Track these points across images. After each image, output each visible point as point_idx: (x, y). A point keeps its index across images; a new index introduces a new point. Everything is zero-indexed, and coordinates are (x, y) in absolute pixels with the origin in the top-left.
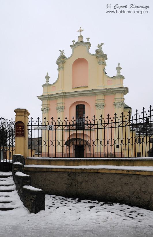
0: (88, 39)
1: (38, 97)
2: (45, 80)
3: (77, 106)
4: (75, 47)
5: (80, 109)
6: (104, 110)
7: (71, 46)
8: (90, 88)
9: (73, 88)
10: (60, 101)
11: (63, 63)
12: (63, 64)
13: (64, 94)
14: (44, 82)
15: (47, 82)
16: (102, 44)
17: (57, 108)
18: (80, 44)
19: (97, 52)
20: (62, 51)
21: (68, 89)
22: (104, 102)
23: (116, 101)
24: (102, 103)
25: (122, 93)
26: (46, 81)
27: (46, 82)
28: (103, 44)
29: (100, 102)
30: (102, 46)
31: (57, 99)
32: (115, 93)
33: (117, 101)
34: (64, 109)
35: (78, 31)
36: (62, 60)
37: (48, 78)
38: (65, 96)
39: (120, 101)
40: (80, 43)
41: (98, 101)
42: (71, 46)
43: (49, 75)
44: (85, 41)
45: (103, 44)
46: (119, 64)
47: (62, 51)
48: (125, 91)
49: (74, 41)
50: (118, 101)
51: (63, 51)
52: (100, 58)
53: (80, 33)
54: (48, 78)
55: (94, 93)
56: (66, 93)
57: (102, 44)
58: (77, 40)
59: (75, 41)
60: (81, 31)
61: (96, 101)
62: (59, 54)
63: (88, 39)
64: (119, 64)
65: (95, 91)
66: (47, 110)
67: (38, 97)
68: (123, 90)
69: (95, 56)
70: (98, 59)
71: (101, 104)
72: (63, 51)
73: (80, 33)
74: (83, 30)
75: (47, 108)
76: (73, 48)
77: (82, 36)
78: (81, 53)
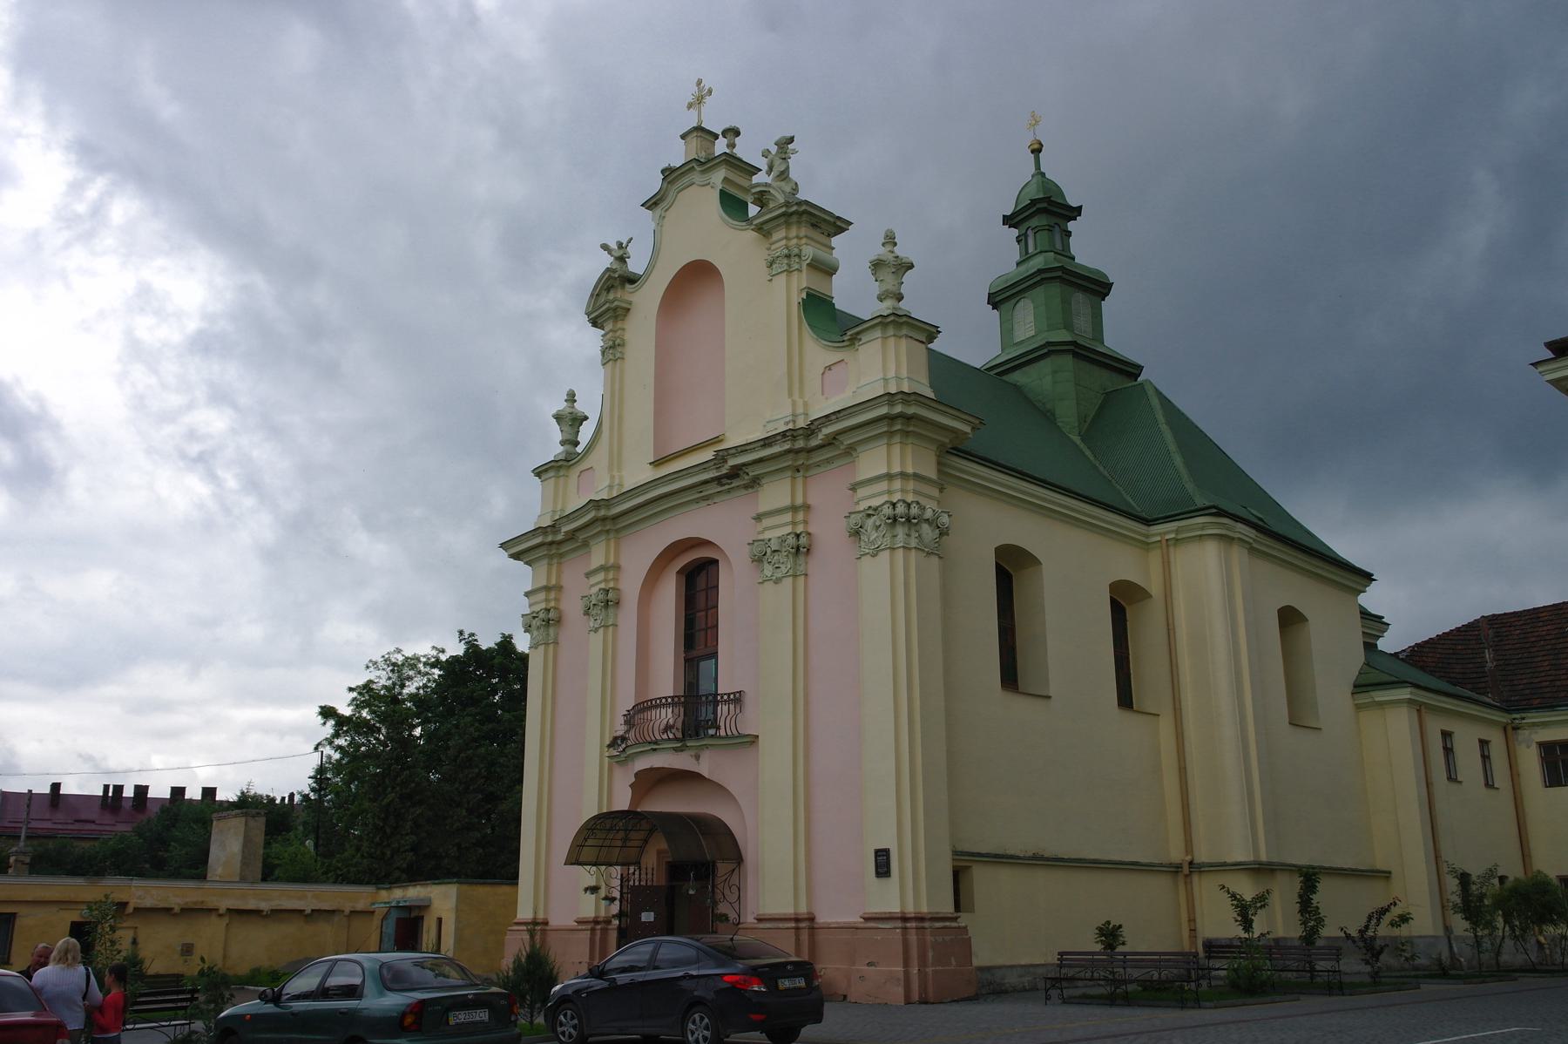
4: (664, 205)
6: (801, 579)
12: (619, 325)
13: (602, 513)
20: (614, 246)
22: (800, 529)
25: (891, 434)
27: (561, 449)
28: (791, 140)
33: (874, 497)
36: (609, 300)
39: (875, 502)
42: (652, 204)
45: (791, 140)
47: (614, 246)
55: (733, 474)
56: (607, 503)
58: (677, 156)
61: (760, 527)
67: (502, 545)
68: (890, 418)
71: (782, 540)
74: (710, 92)
76: (658, 211)
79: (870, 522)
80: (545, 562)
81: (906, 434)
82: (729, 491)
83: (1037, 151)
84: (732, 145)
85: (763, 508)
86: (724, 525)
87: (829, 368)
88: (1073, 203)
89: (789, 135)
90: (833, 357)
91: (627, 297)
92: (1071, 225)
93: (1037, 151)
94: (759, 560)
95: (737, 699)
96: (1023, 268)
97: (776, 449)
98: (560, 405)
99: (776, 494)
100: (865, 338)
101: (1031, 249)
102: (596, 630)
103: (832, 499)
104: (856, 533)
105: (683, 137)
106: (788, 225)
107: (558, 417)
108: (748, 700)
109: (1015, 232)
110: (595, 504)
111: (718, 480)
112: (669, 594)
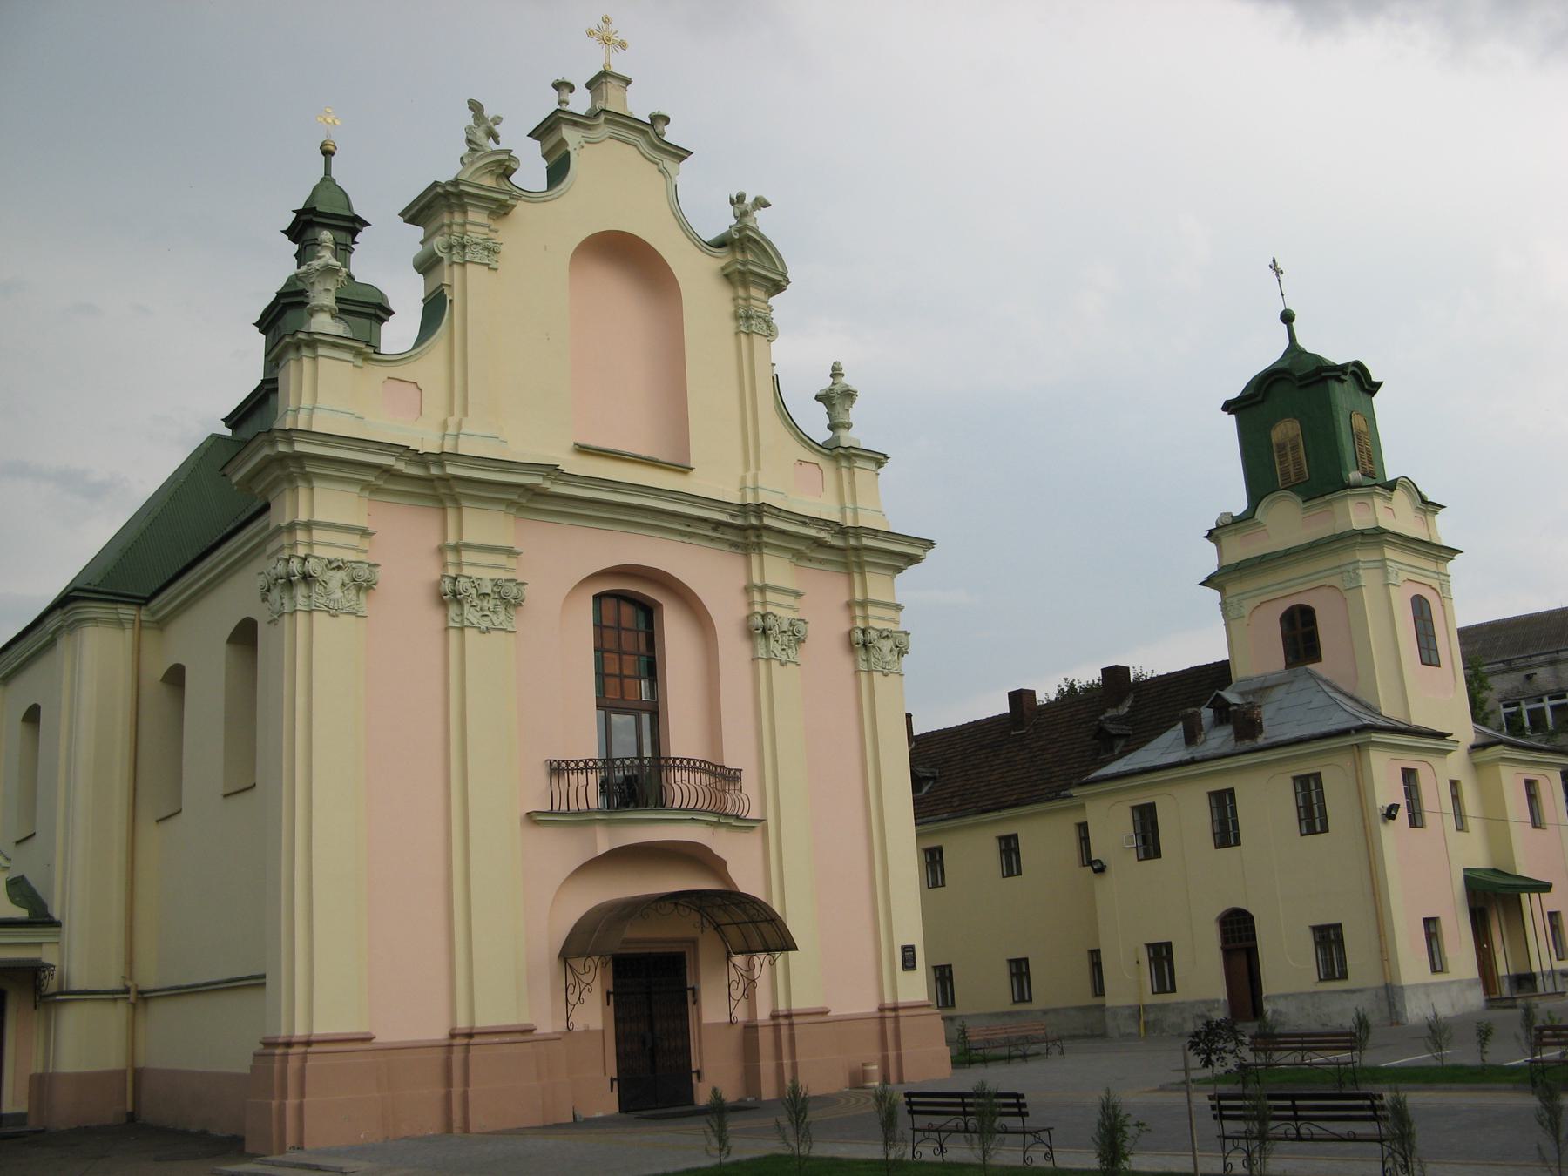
3: (598, 598)
4: (587, 133)
9: (584, 450)
20: (489, 113)
28: (766, 205)
38: (533, 494)
45: (766, 205)
46: (836, 372)
48: (903, 553)
51: (498, 120)
52: (754, 292)
53: (607, 57)
55: (746, 529)
57: (761, 203)
64: (836, 372)
70: (741, 292)
73: (607, 57)
82: (712, 539)
87: (801, 462)
89: (769, 200)
97: (812, 532)
111: (718, 525)
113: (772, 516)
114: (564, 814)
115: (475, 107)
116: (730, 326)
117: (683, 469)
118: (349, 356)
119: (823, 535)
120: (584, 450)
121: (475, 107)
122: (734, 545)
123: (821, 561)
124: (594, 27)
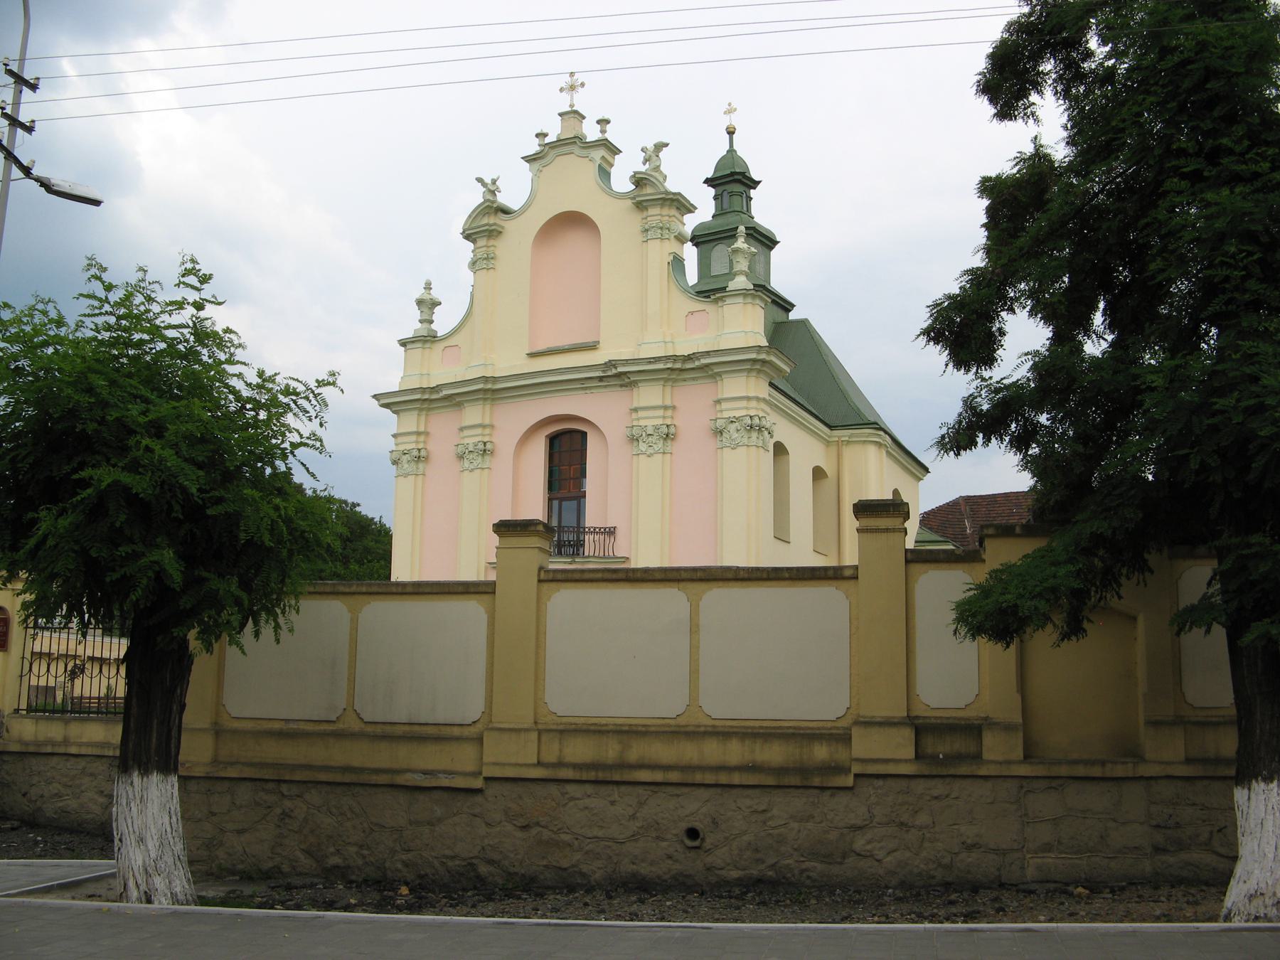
0: (603, 122)
1: (375, 396)
2: (416, 313)
4: (543, 162)
5: (567, 451)
7: (530, 159)
8: (598, 357)
9: (532, 355)
10: (473, 414)
11: (493, 233)
12: (492, 242)
13: (489, 386)
14: (411, 325)
15: (426, 325)
16: (660, 147)
17: (460, 449)
18: (566, 149)
19: (639, 181)
20: (488, 181)
21: (509, 361)
23: (726, 415)
24: (660, 422)
25: (750, 370)
26: (421, 321)
29: (650, 421)
30: (663, 154)
31: (633, 384)
32: (719, 374)
33: (730, 410)
34: (427, 458)
35: (561, 90)
36: (487, 224)
37: (428, 305)
38: (491, 391)
40: (571, 143)
41: (641, 414)
42: (530, 159)
43: (436, 294)
44: (591, 132)
49: (541, 135)
50: (731, 414)
52: (652, 211)
54: (428, 305)
55: (618, 376)
57: (660, 147)
58: (554, 131)
59: (545, 135)
60: (572, 88)
61: (634, 415)
62: (476, 197)
63: (603, 122)
65: (621, 369)
66: (417, 462)
67: (375, 396)
68: (754, 361)
69: (629, 202)
70: (645, 214)
71: (656, 428)
72: (494, 182)
74: (583, 85)
75: (481, 446)
76: (537, 165)
77: (576, 112)
78: (574, 187)
79: (733, 427)
80: (416, 413)
81: (759, 371)
83: (731, 133)
84: (603, 132)
85: (635, 405)
86: (602, 412)
87: (692, 313)
88: (756, 177)
89: (665, 141)
90: (700, 306)
91: (502, 223)
92: (753, 193)
93: (731, 133)
94: (634, 439)
95: (611, 532)
96: (720, 221)
97: (660, 366)
98: (419, 292)
99: (649, 395)
100: (728, 301)
101: (725, 206)
102: (472, 470)
103: (693, 405)
104: (719, 432)
105: (560, 115)
106: (662, 206)
107: (420, 302)
108: (619, 533)
109: (712, 191)
110: (485, 379)
111: (601, 379)
112: (538, 453)
113: (624, 365)
114: (604, 557)
115: (480, 180)
116: (641, 238)
117: (592, 347)
118: (419, 345)
119: (669, 366)
120: (532, 355)
121: (480, 180)
122: (621, 386)
123: (693, 379)
124: (563, 85)
